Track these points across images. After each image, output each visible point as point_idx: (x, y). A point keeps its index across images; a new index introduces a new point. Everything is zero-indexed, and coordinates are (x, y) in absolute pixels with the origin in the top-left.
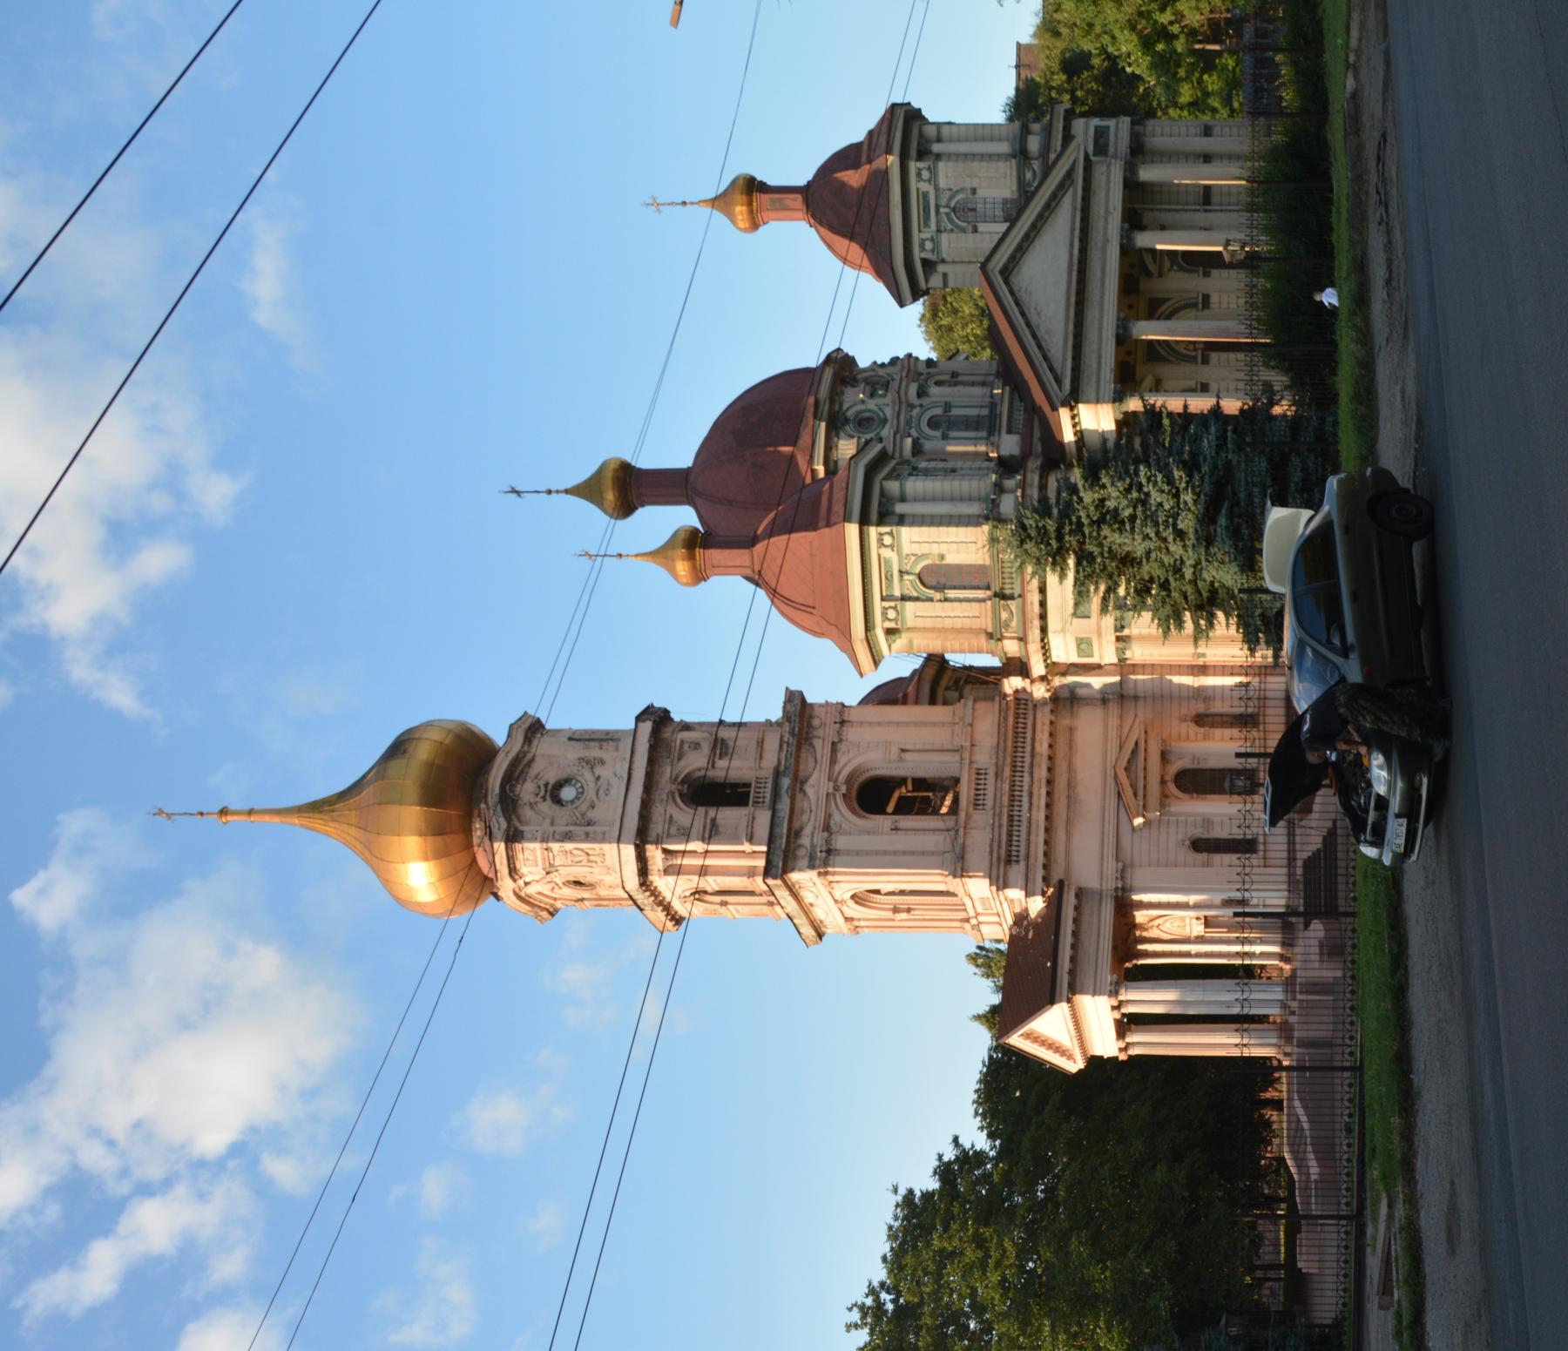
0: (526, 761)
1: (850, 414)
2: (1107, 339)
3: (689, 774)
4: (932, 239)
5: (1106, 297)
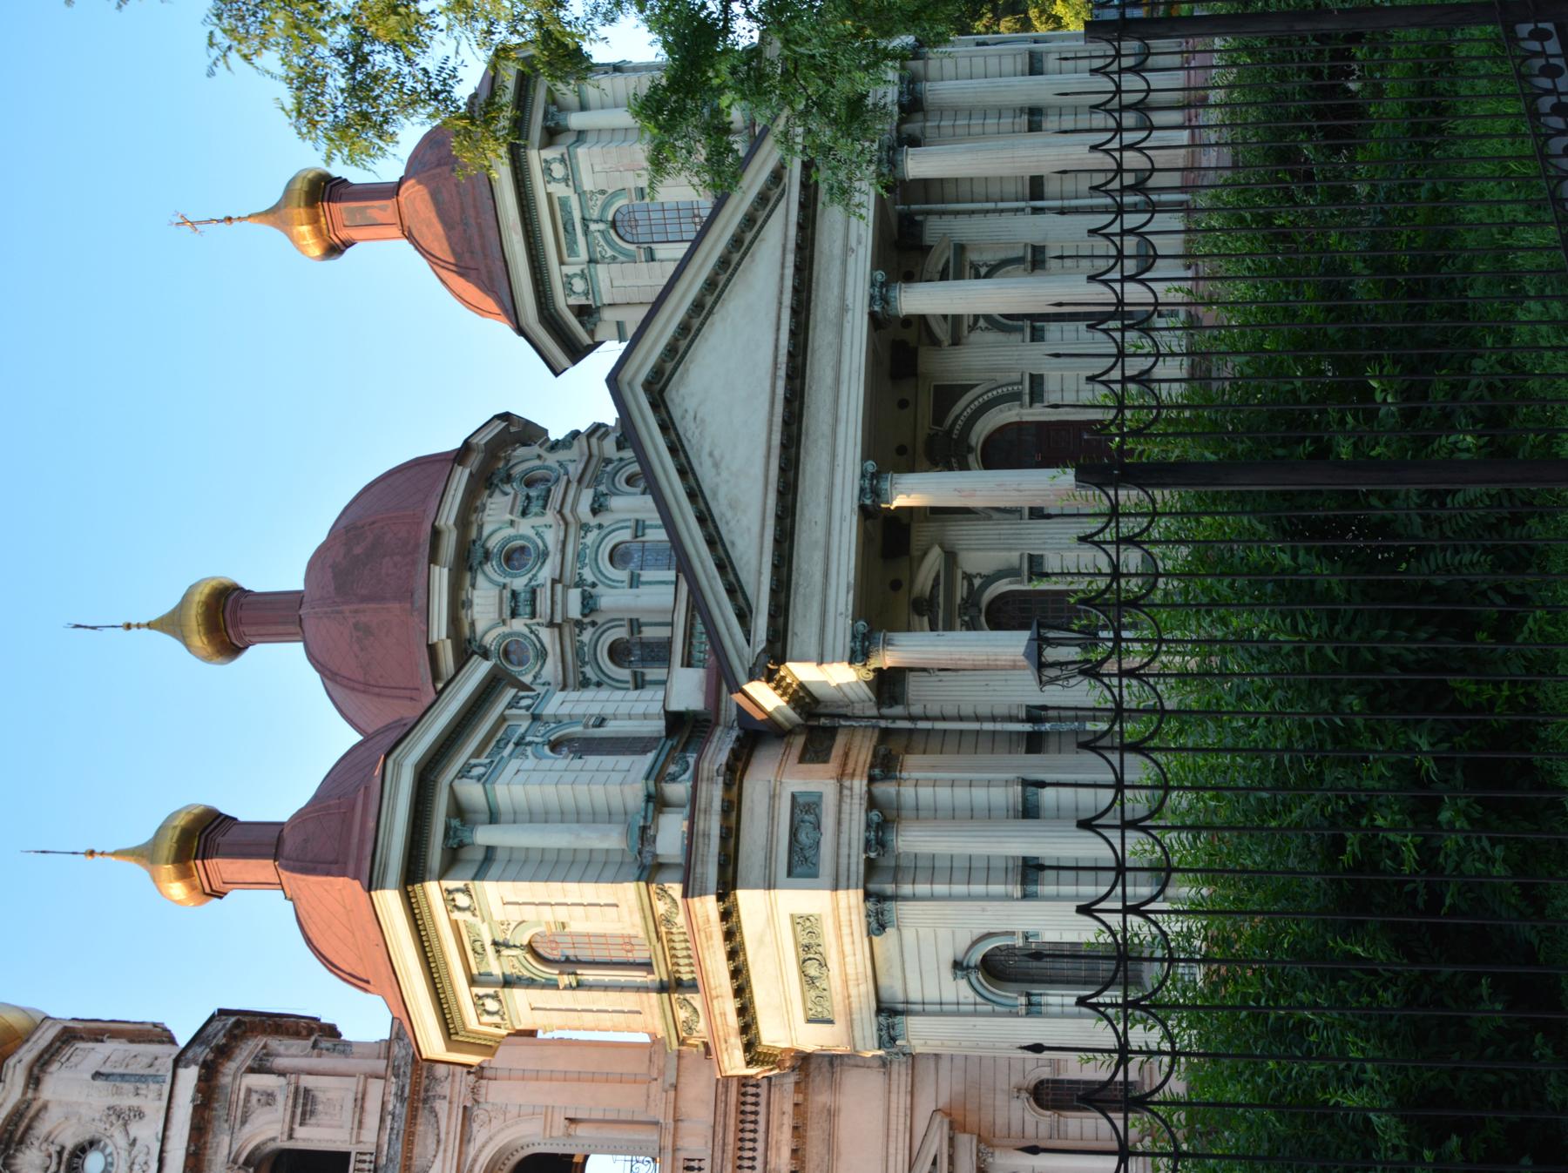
0: (32, 1112)
1: (493, 544)
2: (842, 519)
3: (257, 1148)
4: (582, 275)
5: (841, 429)
